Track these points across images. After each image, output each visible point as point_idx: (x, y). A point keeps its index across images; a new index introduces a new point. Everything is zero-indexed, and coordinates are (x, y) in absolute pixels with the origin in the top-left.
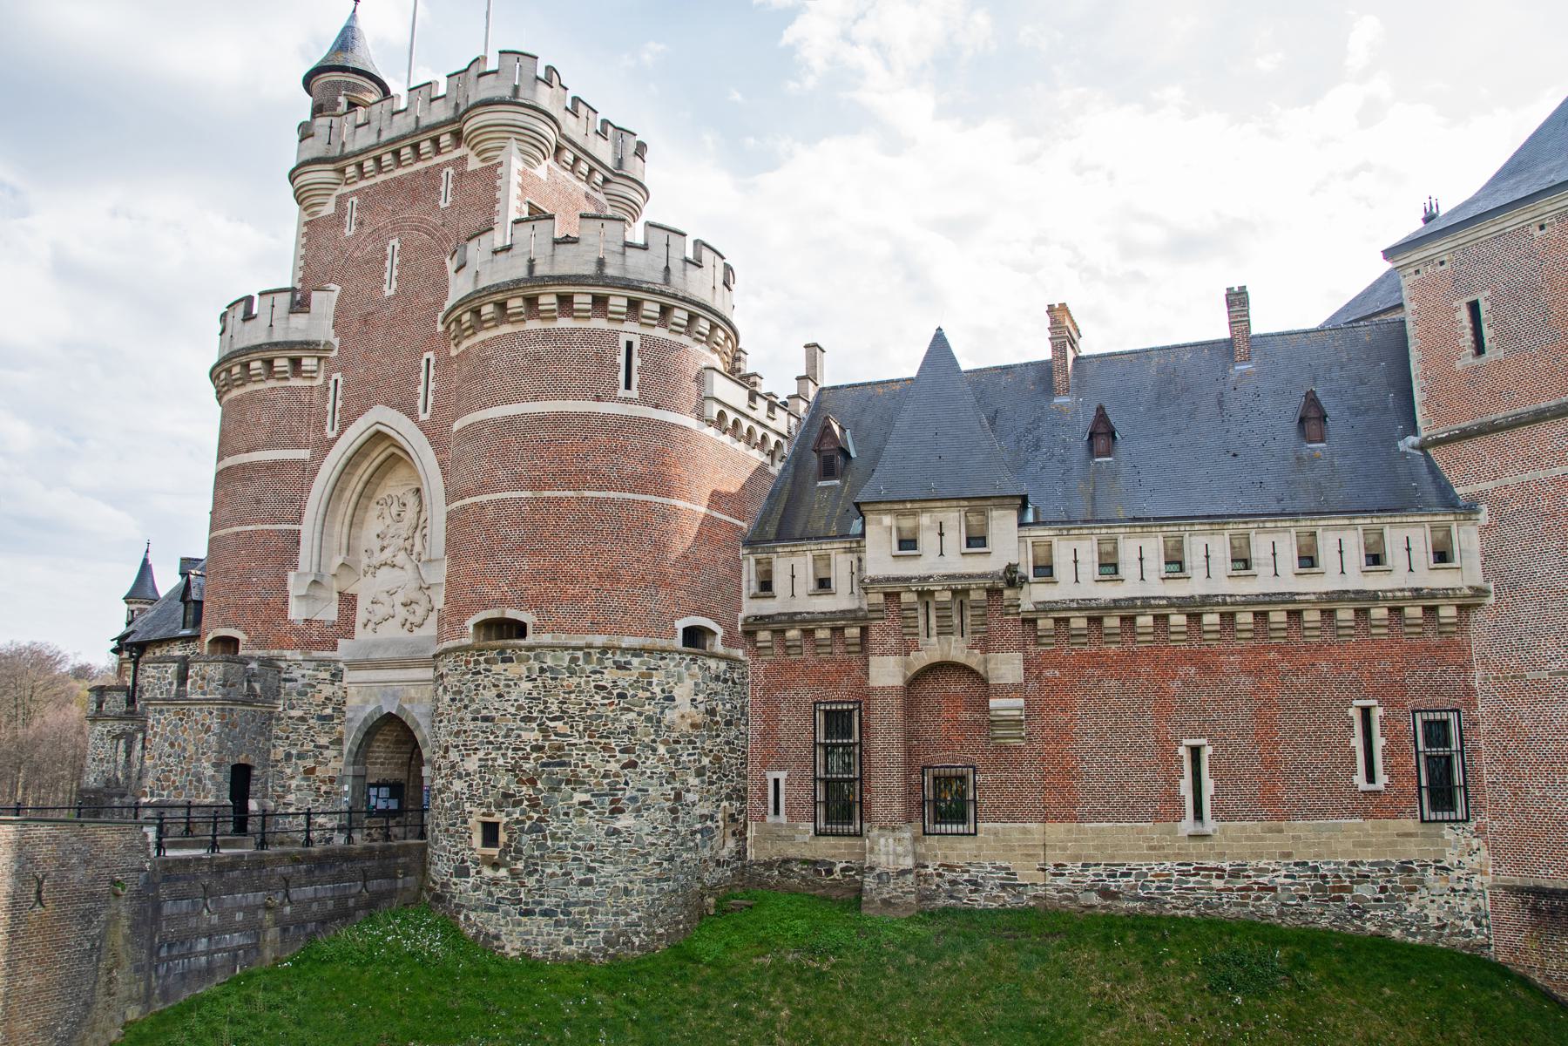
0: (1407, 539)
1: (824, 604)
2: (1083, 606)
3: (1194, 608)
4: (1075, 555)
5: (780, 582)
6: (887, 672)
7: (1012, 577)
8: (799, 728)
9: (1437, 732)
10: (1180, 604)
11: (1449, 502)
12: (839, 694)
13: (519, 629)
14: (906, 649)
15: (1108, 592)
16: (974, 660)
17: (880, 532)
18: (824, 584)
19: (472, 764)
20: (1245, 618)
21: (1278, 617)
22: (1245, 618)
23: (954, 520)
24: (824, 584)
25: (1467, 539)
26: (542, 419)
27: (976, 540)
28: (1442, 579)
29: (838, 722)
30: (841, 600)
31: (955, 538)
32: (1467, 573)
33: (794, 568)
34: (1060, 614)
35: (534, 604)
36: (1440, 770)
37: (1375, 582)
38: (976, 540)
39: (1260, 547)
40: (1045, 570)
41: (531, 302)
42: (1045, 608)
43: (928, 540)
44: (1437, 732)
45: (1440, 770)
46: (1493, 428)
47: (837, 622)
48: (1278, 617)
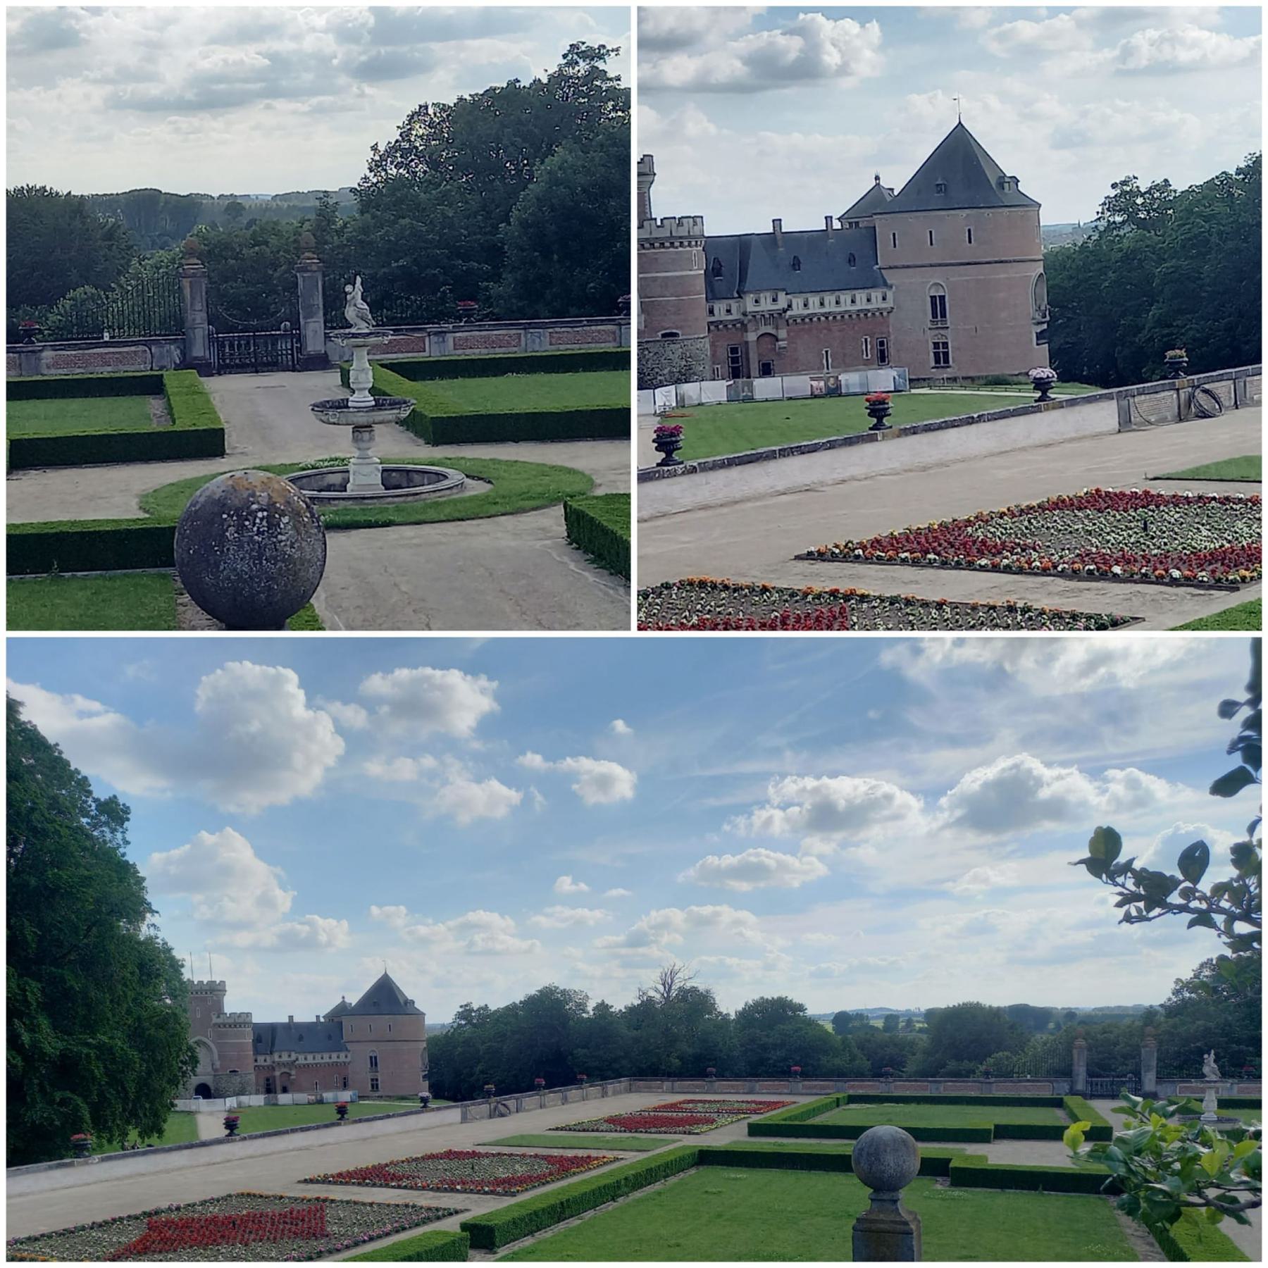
0: (876, 294)
1: (730, 317)
2: (800, 316)
3: (826, 315)
4: (797, 302)
5: (716, 312)
6: (752, 337)
7: (785, 311)
8: (723, 353)
9: (882, 344)
10: (823, 315)
11: (885, 284)
12: (734, 342)
13: (675, 335)
14: (757, 329)
15: (806, 312)
16: (773, 332)
17: (749, 299)
18: (729, 311)
19: (666, 371)
20: (839, 317)
21: (846, 316)
22: (839, 317)
23: (769, 295)
24: (729, 311)
25: (890, 295)
26: (677, 277)
27: (774, 300)
28: (884, 305)
29: (734, 350)
30: (735, 315)
31: (769, 300)
32: (889, 304)
33: (720, 307)
34: (794, 318)
35: (680, 328)
36: (882, 352)
37: (869, 307)
38: (774, 300)
39: (842, 299)
40: (790, 306)
41: (672, 244)
42: (791, 317)
43: (762, 300)
44: (882, 344)
45: (882, 352)
46: (896, 267)
47: (734, 323)
48: (846, 316)
